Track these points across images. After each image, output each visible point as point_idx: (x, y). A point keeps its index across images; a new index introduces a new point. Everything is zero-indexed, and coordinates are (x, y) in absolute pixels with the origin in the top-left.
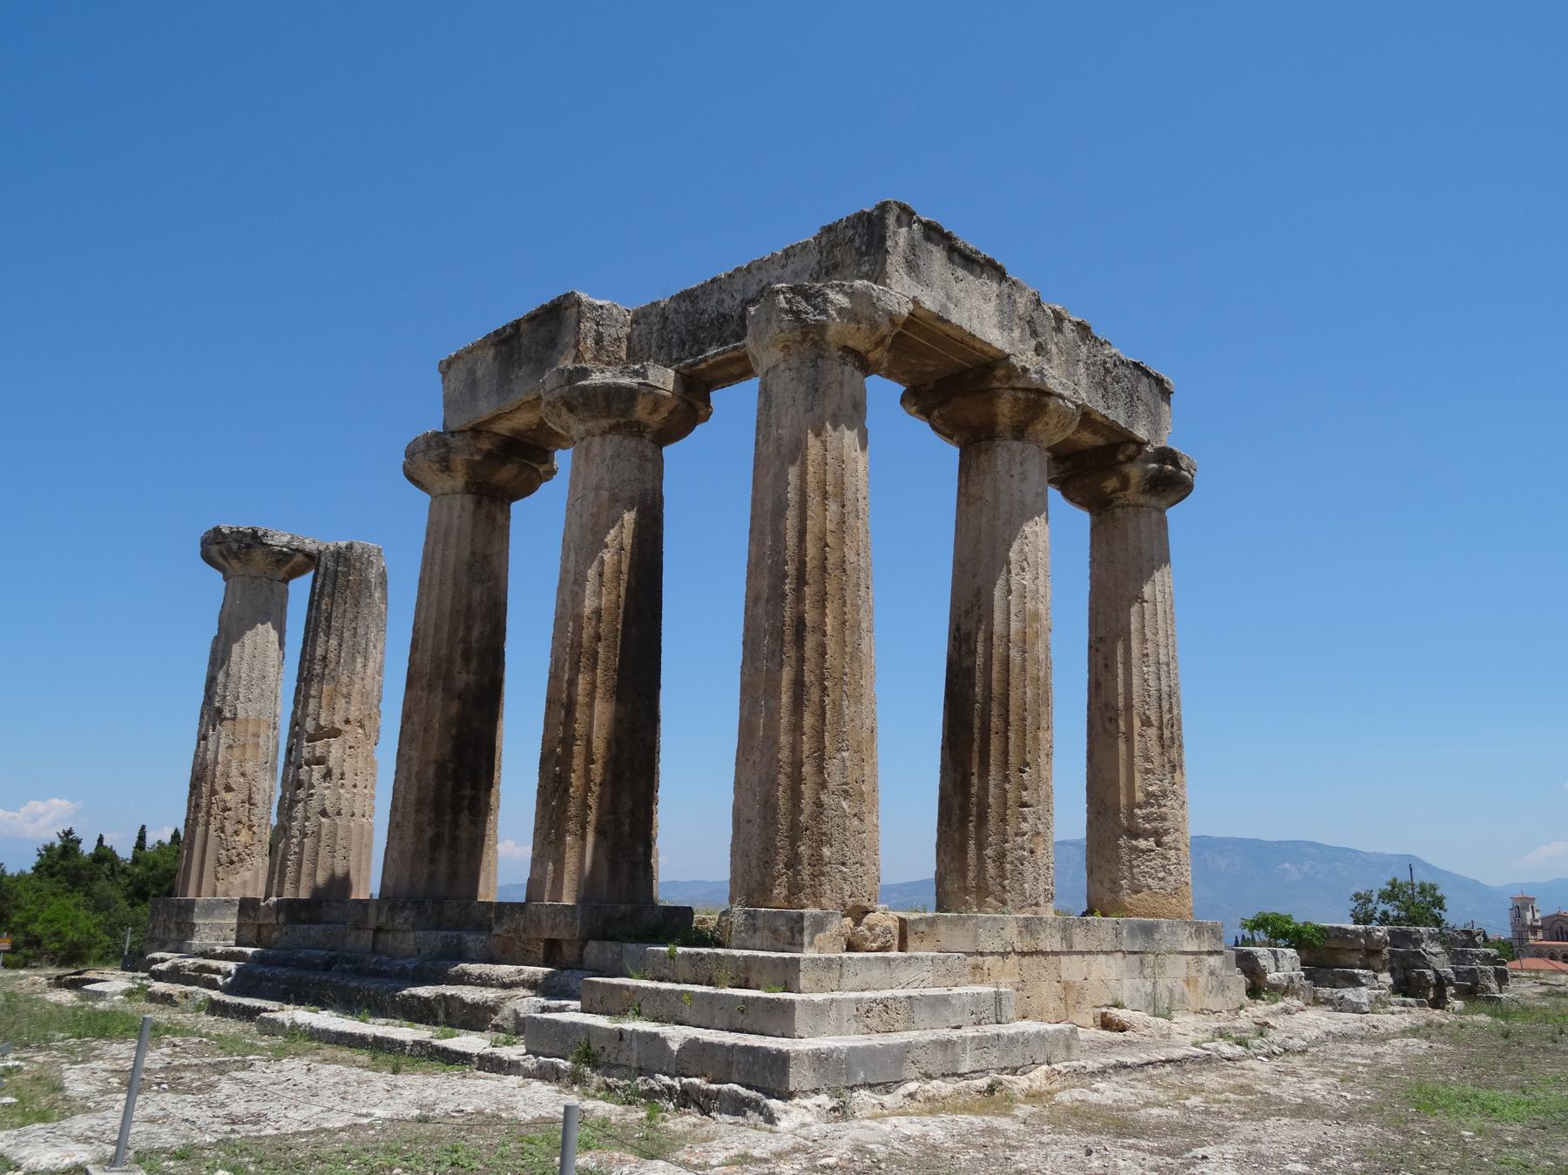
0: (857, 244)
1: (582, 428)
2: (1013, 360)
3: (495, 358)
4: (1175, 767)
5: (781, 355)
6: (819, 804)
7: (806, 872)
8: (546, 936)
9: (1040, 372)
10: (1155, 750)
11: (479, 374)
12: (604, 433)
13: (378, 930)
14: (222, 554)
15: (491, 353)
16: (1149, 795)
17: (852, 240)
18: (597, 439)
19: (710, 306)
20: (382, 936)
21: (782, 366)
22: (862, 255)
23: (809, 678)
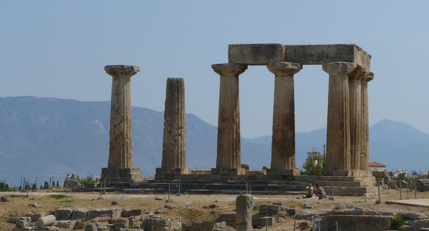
0: (347, 51)
1: (282, 74)
2: (362, 67)
3: (251, 50)
4: (368, 139)
5: (338, 74)
6: (346, 153)
7: (345, 164)
8: (284, 175)
9: (365, 69)
10: (365, 136)
11: (245, 52)
12: (287, 76)
13: (222, 175)
14: (122, 73)
15: (249, 49)
16: (364, 146)
17: (345, 50)
18: (286, 77)
19: (309, 51)
20: (224, 176)
21: (338, 76)
22: (348, 54)
23: (345, 133)
